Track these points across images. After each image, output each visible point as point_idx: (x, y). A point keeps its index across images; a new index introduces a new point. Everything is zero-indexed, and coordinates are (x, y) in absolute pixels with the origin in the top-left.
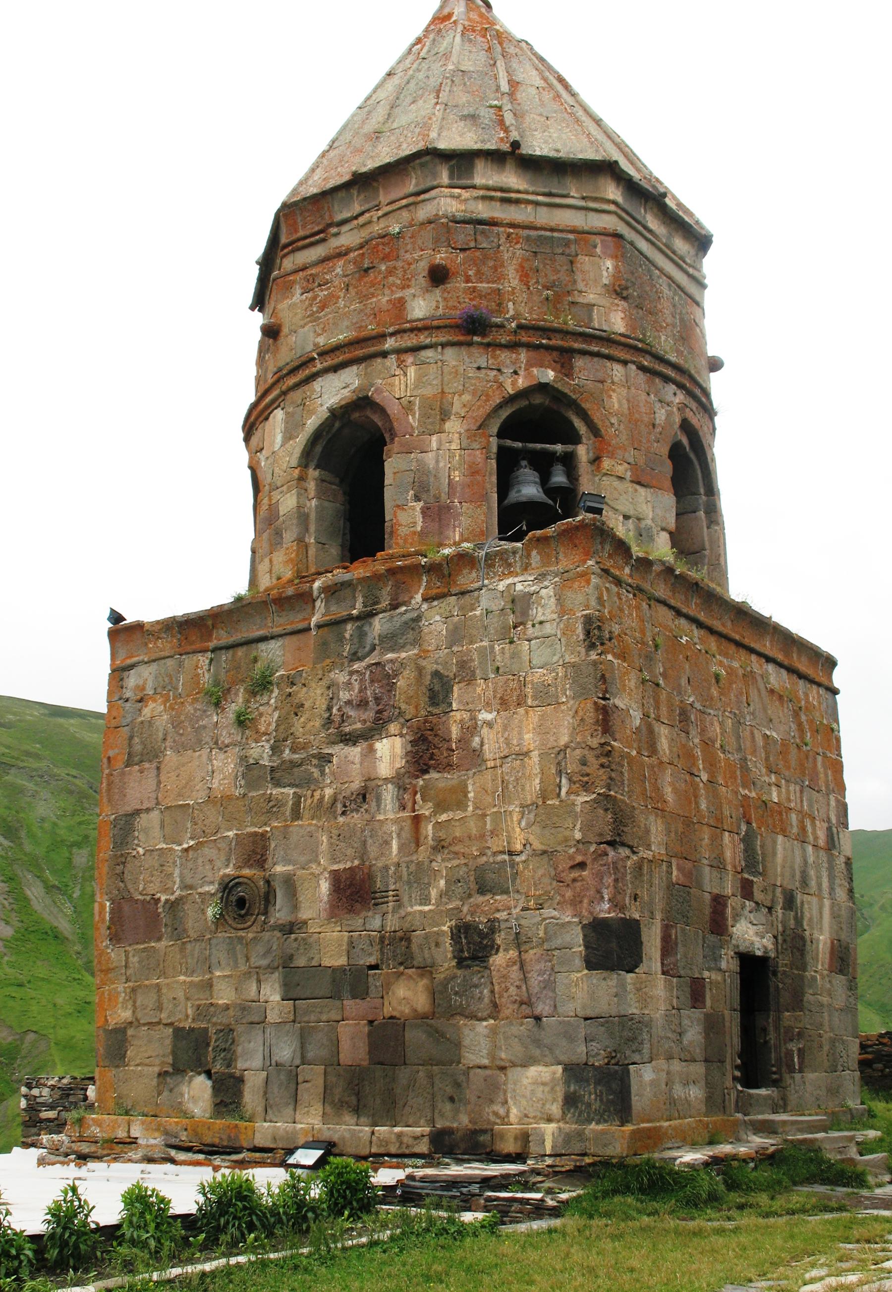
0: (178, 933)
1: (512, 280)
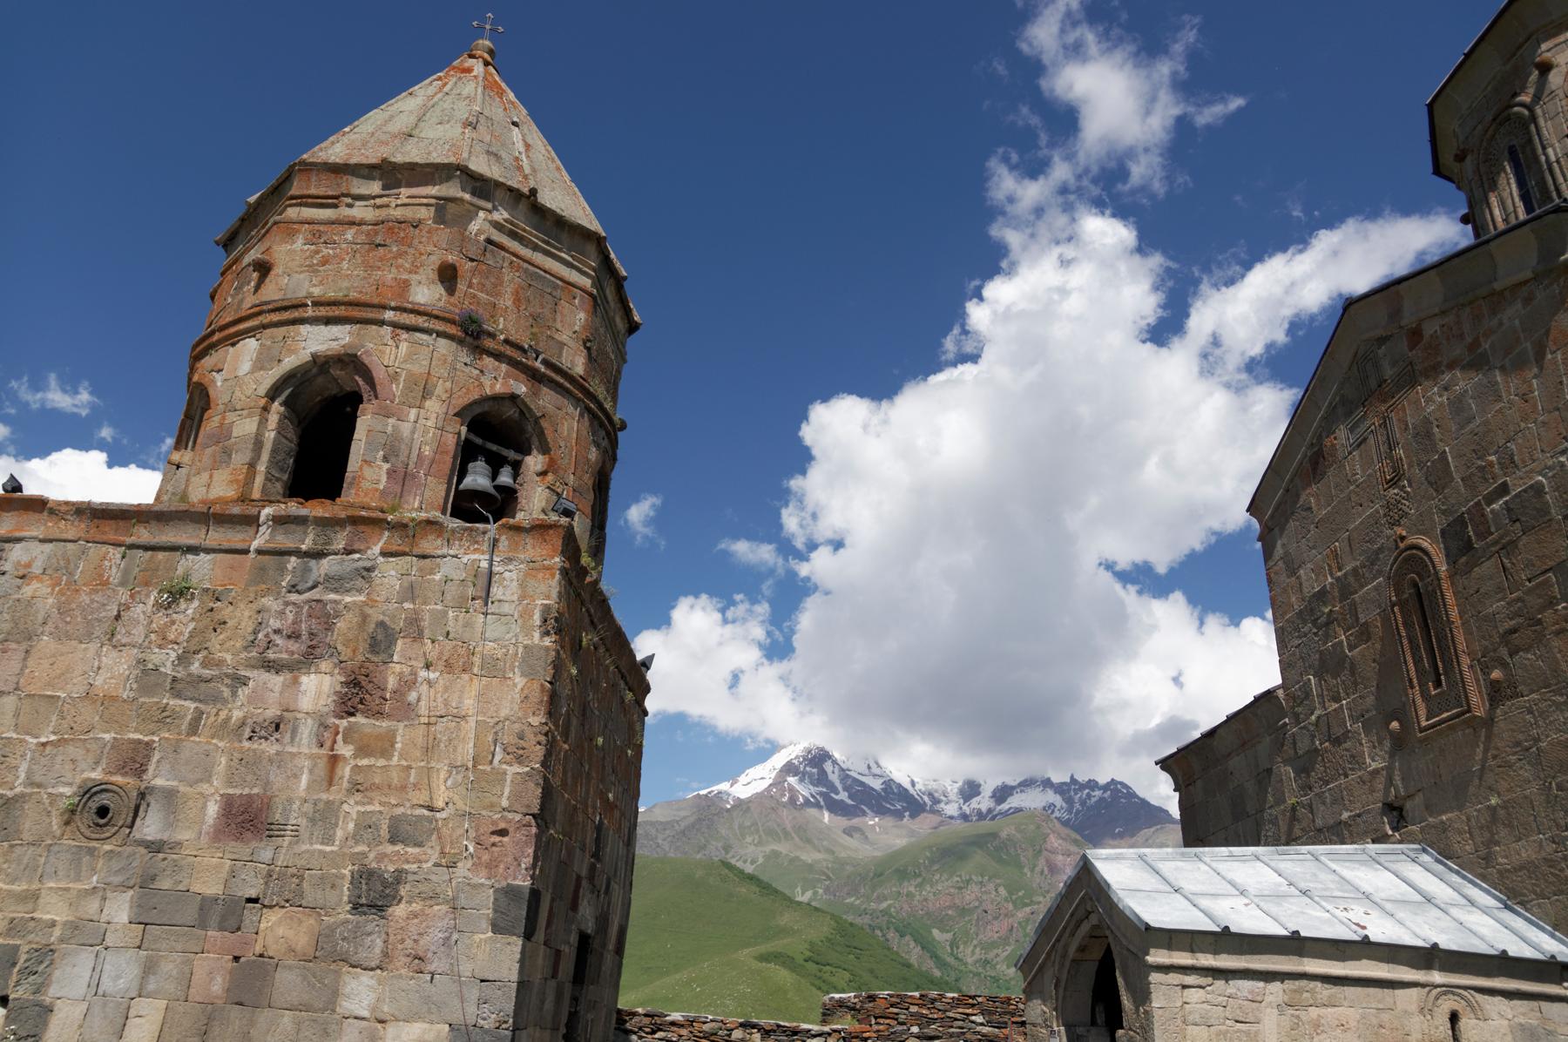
1: (507, 301)
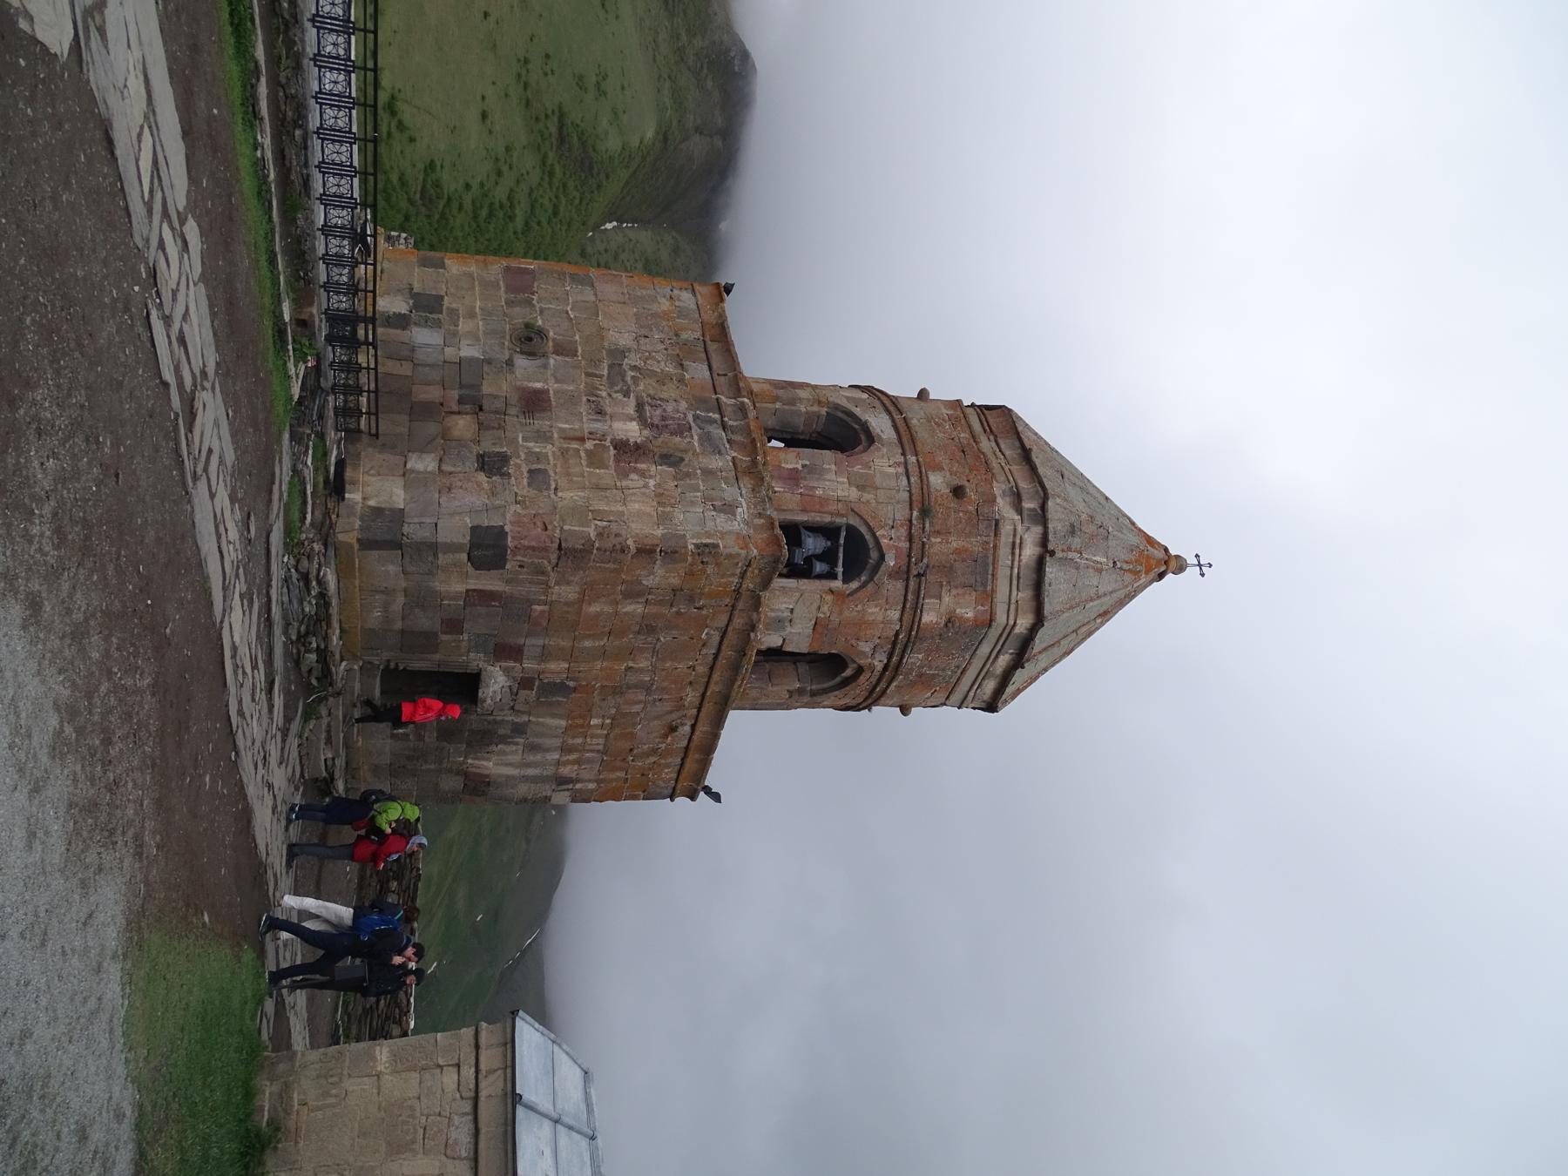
1: (956, 543)
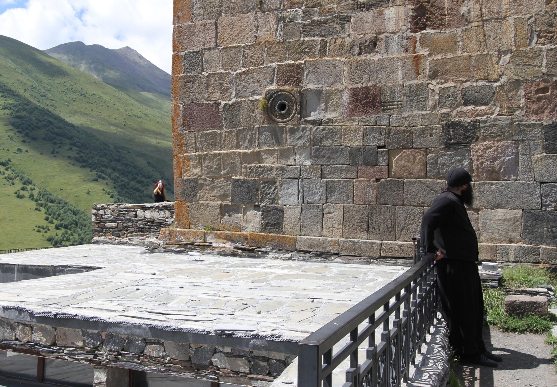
0: (234, 123)
